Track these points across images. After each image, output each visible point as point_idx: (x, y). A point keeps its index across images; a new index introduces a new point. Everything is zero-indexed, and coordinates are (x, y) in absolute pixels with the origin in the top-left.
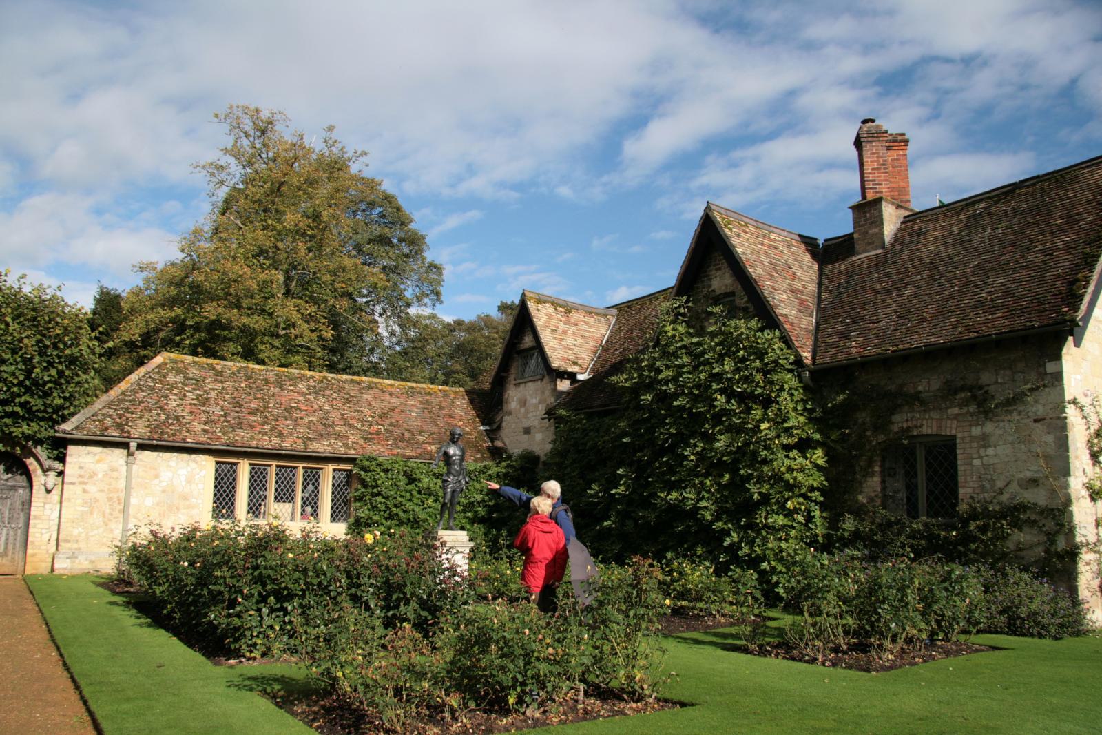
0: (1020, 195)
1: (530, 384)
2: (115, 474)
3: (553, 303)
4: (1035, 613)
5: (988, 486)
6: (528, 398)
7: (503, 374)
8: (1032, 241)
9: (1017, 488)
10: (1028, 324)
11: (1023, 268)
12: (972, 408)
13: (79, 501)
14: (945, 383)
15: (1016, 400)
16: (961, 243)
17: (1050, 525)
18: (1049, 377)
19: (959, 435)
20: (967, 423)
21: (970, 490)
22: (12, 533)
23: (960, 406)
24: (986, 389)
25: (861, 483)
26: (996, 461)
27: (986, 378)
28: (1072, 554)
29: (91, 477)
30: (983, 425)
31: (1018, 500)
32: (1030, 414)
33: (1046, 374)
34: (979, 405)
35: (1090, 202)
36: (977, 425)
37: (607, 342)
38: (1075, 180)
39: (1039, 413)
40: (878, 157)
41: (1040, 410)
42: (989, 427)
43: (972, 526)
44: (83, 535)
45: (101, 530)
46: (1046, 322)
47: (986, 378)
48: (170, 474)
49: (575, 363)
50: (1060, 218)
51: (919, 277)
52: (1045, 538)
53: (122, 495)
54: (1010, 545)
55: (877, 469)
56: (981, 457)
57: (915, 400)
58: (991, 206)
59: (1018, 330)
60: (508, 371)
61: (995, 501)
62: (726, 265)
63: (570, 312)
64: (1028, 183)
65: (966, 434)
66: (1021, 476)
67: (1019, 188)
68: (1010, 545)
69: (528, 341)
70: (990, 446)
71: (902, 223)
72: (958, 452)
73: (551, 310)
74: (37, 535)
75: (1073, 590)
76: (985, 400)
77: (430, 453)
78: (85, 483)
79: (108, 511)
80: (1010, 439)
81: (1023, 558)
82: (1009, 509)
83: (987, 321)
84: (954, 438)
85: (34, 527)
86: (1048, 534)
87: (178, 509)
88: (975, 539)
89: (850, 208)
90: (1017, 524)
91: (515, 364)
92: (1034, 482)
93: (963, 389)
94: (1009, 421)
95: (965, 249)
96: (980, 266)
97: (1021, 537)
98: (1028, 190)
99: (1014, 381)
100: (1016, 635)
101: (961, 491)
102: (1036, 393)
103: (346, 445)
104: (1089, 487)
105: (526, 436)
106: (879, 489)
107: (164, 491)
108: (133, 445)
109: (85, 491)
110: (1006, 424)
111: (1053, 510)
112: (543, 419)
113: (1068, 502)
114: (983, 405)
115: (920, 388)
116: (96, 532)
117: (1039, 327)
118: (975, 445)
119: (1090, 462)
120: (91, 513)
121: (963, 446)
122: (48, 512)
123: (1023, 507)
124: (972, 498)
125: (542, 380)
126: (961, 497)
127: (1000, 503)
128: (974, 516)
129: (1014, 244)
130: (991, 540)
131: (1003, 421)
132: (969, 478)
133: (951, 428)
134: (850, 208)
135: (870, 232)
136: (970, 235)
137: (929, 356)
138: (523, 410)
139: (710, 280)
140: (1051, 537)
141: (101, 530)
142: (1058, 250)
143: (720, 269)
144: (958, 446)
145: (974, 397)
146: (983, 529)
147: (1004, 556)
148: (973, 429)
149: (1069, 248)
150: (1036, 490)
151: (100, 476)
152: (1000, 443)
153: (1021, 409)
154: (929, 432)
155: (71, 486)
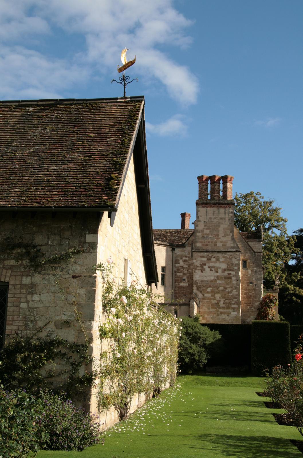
0: (60, 109)
4: (67, 429)
5: (31, 325)
8: (74, 144)
9: (54, 328)
10: (79, 203)
11: (70, 162)
14: (6, 239)
15: (64, 258)
16: (17, 133)
17: (75, 357)
18: (87, 245)
19: (11, 282)
20: (19, 273)
21: (15, 328)
23: (17, 259)
24: (38, 248)
26: (39, 305)
27: (39, 239)
28: (89, 380)
30: (32, 276)
31: (53, 337)
32: (70, 271)
33: (85, 242)
34: (31, 260)
35: (113, 127)
36: (28, 275)
38: (99, 109)
39: (76, 272)
41: (78, 269)
42: (37, 278)
43: (19, 357)
46: (93, 204)
47: (39, 239)
50: (92, 132)
52: (71, 367)
54: (43, 373)
56: (28, 302)
58: (39, 111)
59: (72, 207)
61: (35, 337)
64: (66, 102)
65: (17, 282)
66: (58, 318)
67: (60, 104)
68: (43, 373)
70: (36, 293)
72: (9, 296)
75: (87, 408)
76: (37, 256)
80: (53, 289)
81: (52, 383)
82: (46, 344)
83: (45, 196)
84: (7, 284)
86: (72, 364)
88: (17, 368)
90: (50, 357)
92: (67, 323)
93: (19, 246)
94: (54, 275)
95: (21, 138)
96: (35, 154)
97: (53, 366)
98: (67, 107)
99: (61, 245)
100: (52, 449)
101: (8, 328)
102: (77, 256)
104: (101, 330)
110: (51, 278)
111: (78, 346)
113: (91, 340)
114: (35, 261)
117: (88, 207)
118: (24, 291)
119: (102, 311)
121: (13, 291)
123: (57, 343)
124: (17, 334)
126: (7, 332)
127: (38, 339)
128: (18, 348)
129: (61, 143)
130: (29, 368)
131: (49, 275)
132: (15, 318)
136: (24, 128)
140: (75, 366)
142: (94, 154)
145: (28, 253)
146: (24, 360)
147: (39, 382)
148: (24, 279)
149: (103, 155)
150: (67, 330)
152: (45, 291)
153: (64, 266)
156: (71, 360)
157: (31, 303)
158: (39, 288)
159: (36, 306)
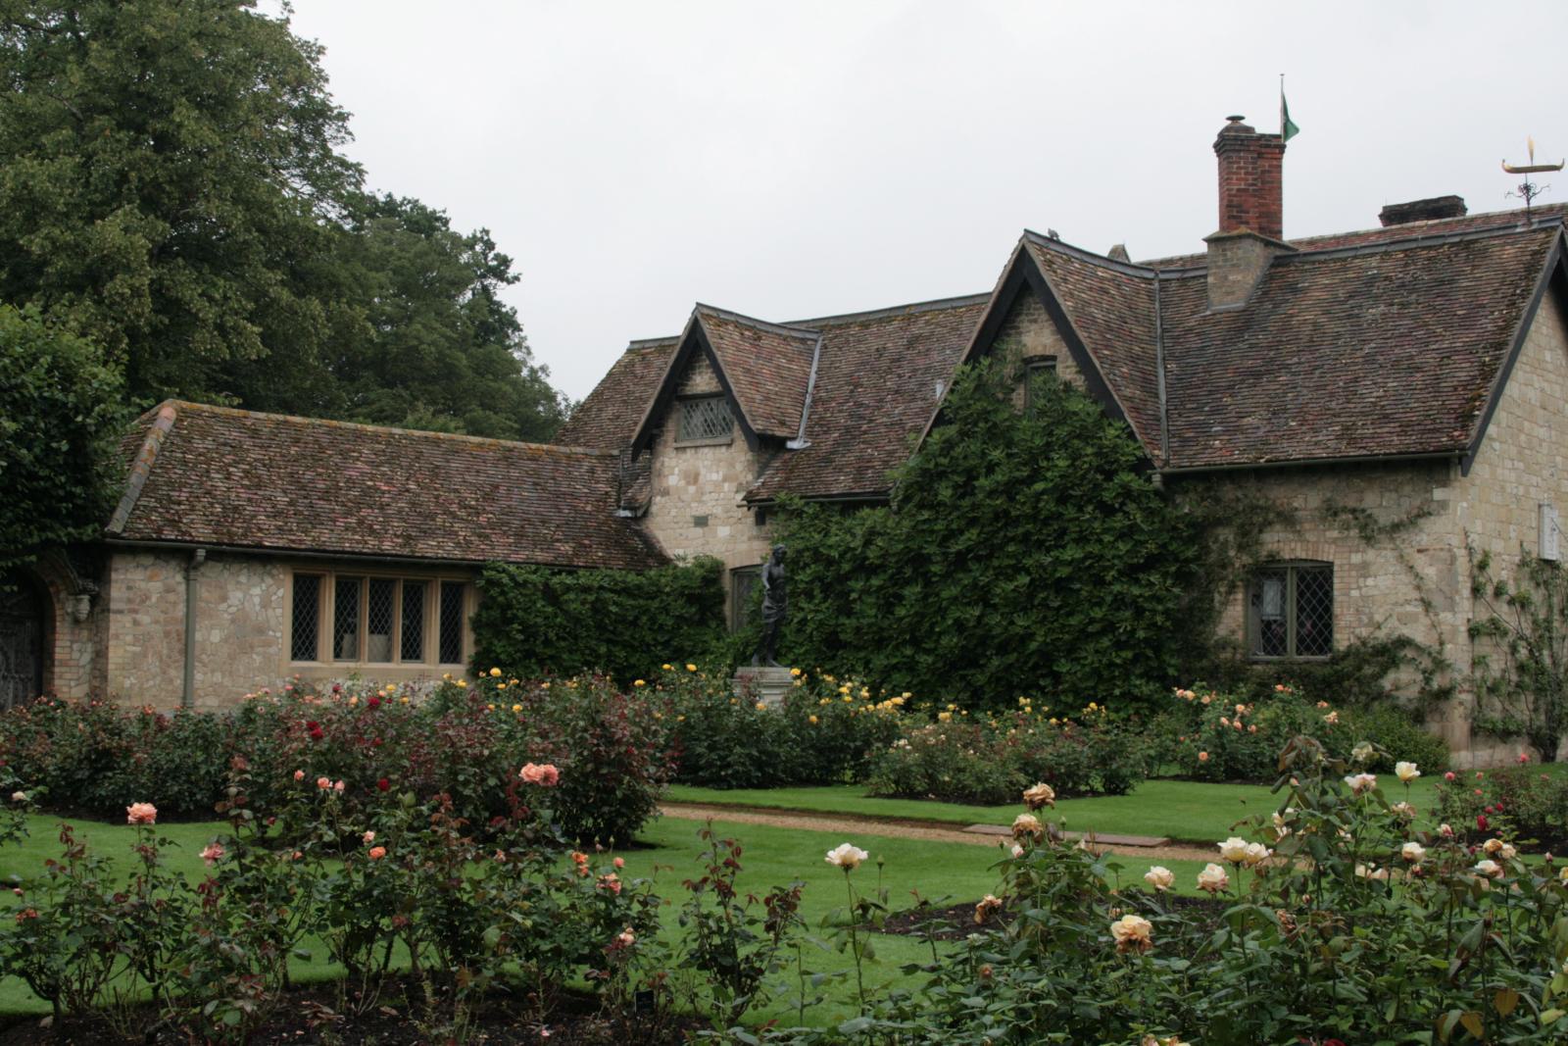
1: (706, 450)
2: (171, 597)
3: (737, 324)
6: (703, 471)
7: (655, 431)
9: (1397, 623)
12: (1354, 532)
13: (129, 638)
19: (1337, 562)
22: (20, 687)
25: (1220, 612)
29: (143, 601)
36: (1358, 551)
37: (816, 387)
40: (1246, 173)
42: (1371, 555)
44: (136, 688)
45: (158, 680)
48: (240, 595)
49: (783, 423)
51: (1295, 360)
52: (1421, 677)
53: (182, 628)
55: (1240, 596)
56: (1359, 588)
57: (1288, 519)
60: (663, 425)
62: (1044, 316)
63: (760, 338)
69: (702, 382)
71: (1272, 266)
72: (1335, 580)
73: (736, 336)
74: (65, 689)
77: (565, 556)
78: (135, 611)
79: (165, 652)
80: (1392, 569)
84: (1330, 565)
85: (60, 678)
86: (1424, 672)
87: (252, 647)
89: (1206, 240)
91: (674, 416)
103: (458, 544)
105: (699, 531)
106: (1241, 620)
107: (233, 621)
108: (201, 553)
109: (136, 623)
114: (1369, 532)
115: (1295, 505)
116: (151, 683)
118: (1354, 573)
120: (145, 656)
122: (76, 655)
125: (729, 445)
133: (1327, 554)
134: (1206, 240)
135: (1231, 278)
137: (1309, 471)
138: (692, 489)
139: (1020, 334)
141: (158, 680)
143: (1035, 321)
144: (1335, 574)
149: (1469, 350)
151: (154, 600)
154: (1304, 556)
155: (119, 616)
156: (1422, 666)
157: (1364, 590)
158: (1373, 569)
159: (1370, 593)
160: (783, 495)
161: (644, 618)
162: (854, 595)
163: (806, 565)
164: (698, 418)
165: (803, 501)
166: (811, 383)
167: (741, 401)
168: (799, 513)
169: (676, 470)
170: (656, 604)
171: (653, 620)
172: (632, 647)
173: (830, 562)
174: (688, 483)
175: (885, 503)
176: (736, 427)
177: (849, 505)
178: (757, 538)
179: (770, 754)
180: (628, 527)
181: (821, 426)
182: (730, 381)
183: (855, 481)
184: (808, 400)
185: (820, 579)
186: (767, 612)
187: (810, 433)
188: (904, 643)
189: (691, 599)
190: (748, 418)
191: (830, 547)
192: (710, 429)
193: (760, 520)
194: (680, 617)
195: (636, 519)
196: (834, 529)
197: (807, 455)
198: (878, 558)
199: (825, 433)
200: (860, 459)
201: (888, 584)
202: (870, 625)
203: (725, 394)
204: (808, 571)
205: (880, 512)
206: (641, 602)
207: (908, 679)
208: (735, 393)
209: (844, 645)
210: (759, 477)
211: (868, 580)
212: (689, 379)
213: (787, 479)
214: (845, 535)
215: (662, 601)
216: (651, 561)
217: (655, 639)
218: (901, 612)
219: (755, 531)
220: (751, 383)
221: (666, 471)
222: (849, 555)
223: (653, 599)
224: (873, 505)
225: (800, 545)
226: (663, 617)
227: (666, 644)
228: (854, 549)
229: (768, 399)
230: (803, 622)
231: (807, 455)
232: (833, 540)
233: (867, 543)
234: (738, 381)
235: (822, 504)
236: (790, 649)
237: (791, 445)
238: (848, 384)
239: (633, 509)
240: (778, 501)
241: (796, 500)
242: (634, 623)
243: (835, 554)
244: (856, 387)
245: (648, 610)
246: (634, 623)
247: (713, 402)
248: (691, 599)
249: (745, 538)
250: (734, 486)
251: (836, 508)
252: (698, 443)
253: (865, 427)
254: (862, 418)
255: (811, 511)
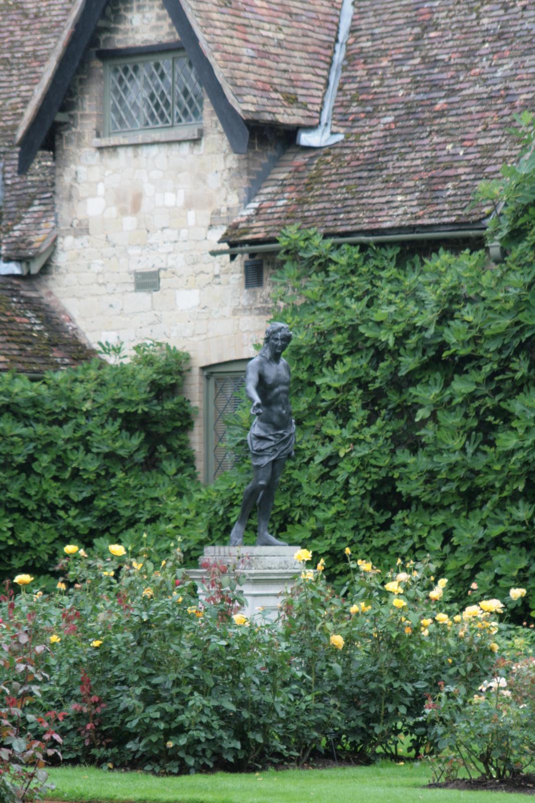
1: (154, 150)
6: (149, 190)
7: (60, 117)
37: (352, 31)
49: (292, 100)
105: (144, 297)
112: (214, 253)
125: (196, 141)
138: (129, 222)
160: (292, 231)
161: (45, 459)
162: (422, 414)
163: (336, 358)
164: (138, 92)
165: (329, 242)
166: (345, 24)
167: (215, 59)
168: (323, 265)
169: (101, 188)
170: (66, 432)
171: (61, 461)
172: (24, 511)
173: (379, 353)
174: (123, 212)
175: (477, 244)
176: (208, 109)
177: (414, 248)
178: (248, 309)
179: (256, 708)
180: (15, 292)
181: (362, 103)
182: (195, 22)
183: (423, 203)
184: (339, 56)
185: (362, 384)
186: (257, 445)
187: (342, 118)
188: (515, 497)
189: (131, 422)
190: (228, 90)
191: (379, 324)
192: (160, 111)
193: (254, 274)
194: (110, 456)
195: (27, 278)
196: (385, 291)
197: (337, 158)
198: (466, 343)
199: (369, 115)
200: (431, 162)
201: (484, 390)
202: (452, 468)
203: (185, 45)
204: (340, 369)
205: (467, 260)
206: (40, 429)
207: (523, 564)
208: (203, 45)
209: (406, 503)
210: (249, 201)
211: (447, 384)
212: (118, 18)
213: (301, 202)
214: (405, 302)
215: (79, 426)
216: (57, 355)
217: (66, 497)
218: (507, 441)
219: (243, 297)
220: (232, 26)
221: (82, 190)
222: (412, 341)
223: (61, 423)
224: (455, 246)
225: (325, 322)
226: (81, 455)
227: (85, 505)
228: (423, 329)
229: (265, 55)
230: (331, 462)
231: (337, 158)
232: (383, 312)
233: (445, 317)
234: (208, 23)
235: (364, 247)
236: (309, 510)
237: (306, 139)
238: (412, 23)
239: (20, 260)
240: (283, 243)
241: (317, 240)
242: (26, 468)
243: (388, 338)
244: (425, 29)
245: (51, 444)
246: (26, 468)
247: (165, 62)
248: (131, 422)
249: (227, 311)
250: (205, 217)
251: (392, 253)
252: (140, 138)
253: (441, 104)
254: (435, 86)
255: (343, 260)
